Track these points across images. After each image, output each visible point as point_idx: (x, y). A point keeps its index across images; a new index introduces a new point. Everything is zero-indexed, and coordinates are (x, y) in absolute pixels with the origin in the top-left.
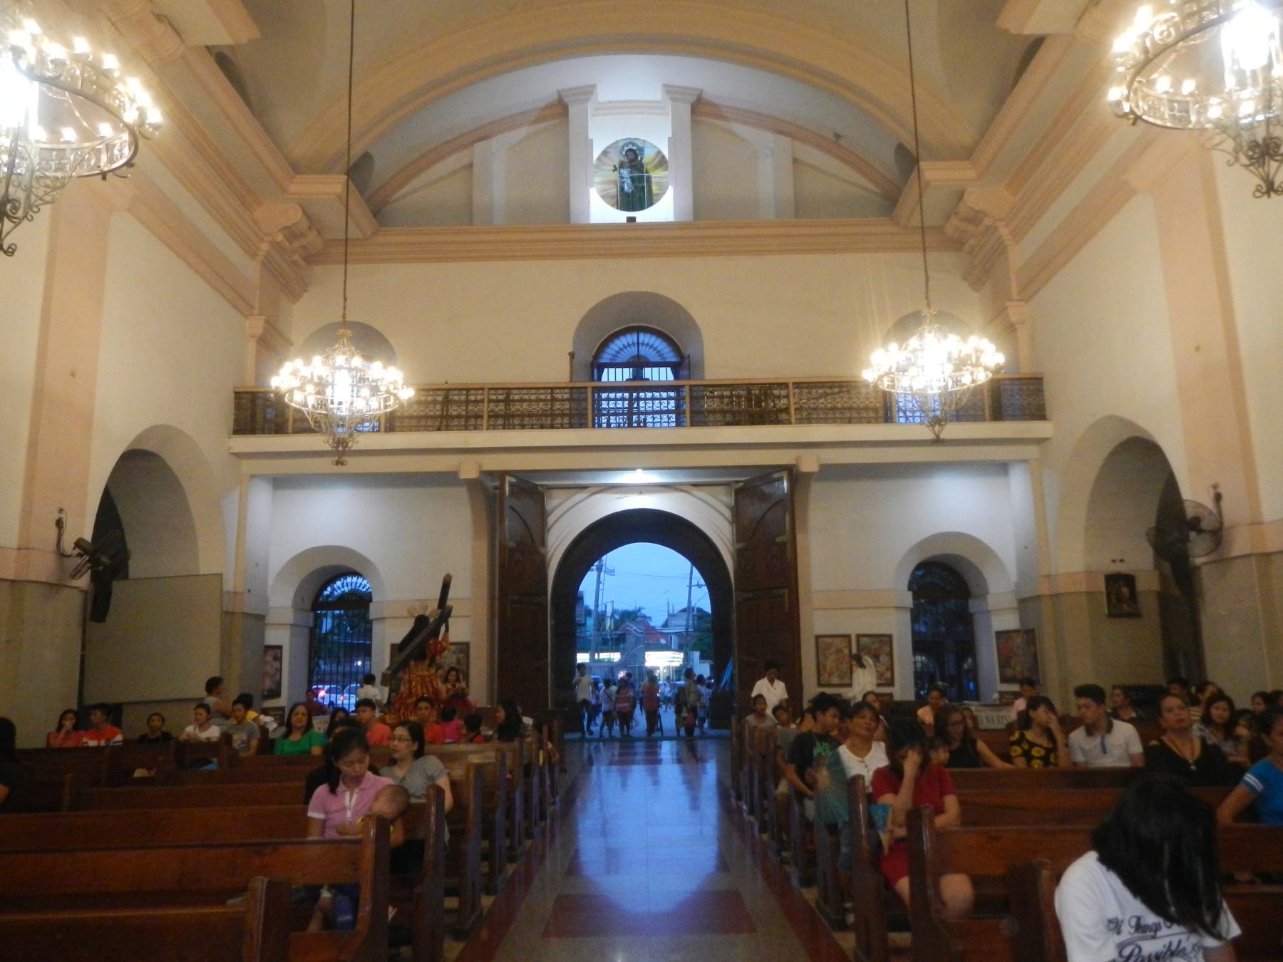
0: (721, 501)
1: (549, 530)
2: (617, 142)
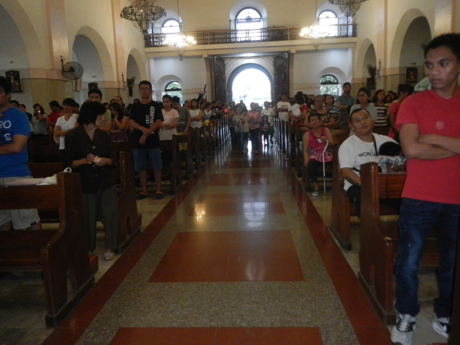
0: (271, 60)
1: (226, 69)
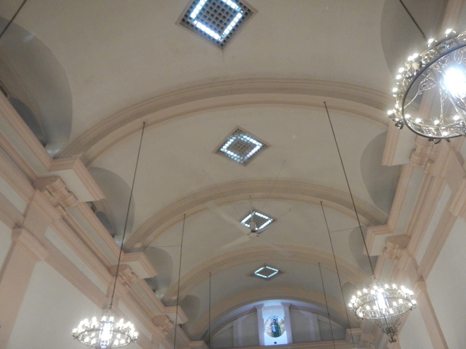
2: (270, 317)
